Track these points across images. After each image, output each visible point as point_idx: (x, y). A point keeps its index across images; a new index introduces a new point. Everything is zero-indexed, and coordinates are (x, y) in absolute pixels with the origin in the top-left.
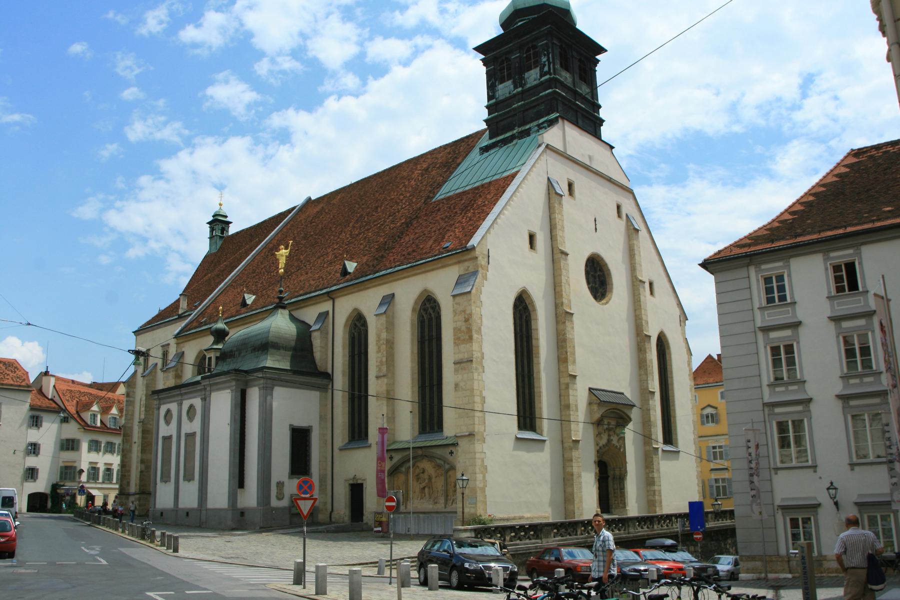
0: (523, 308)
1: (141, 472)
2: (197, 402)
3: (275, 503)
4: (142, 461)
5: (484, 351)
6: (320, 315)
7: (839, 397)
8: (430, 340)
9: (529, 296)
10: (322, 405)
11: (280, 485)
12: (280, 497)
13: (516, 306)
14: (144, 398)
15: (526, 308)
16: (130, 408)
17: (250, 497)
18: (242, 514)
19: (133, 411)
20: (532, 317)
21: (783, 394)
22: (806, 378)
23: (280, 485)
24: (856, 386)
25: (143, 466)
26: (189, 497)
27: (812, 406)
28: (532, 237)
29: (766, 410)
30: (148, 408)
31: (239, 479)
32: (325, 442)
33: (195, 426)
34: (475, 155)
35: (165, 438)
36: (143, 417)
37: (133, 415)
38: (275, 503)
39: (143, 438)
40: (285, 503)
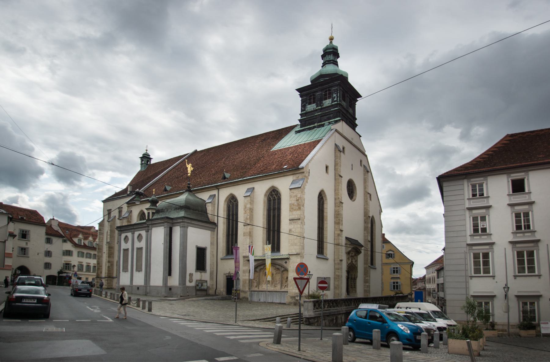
0: (321, 197)
1: (109, 267)
2: (143, 233)
3: (188, 284)
4: (109, 262)
5: (305, 215)
6: (211, 196)
7: (511, 242)
8: (274, 209)
9: (324, 193)
10: (212, 238)
11: (191, 275)
12: (191, 281)
13: (319, 197)
14: (109, 232)
15: (322, 198)
16: (101, 236)
17: (174, 281)
18: (170, 289)
19: (103, 238)
20: (325, 202)
21: (478, 240)
22: (491, 233)
23: (191, 275)
24: (520, 237)
25: (109, 264)
26: (139, 279)
27: (495, 247)
28: (327, 167)
29: (468, 247)
30: (112, 236)
31: (169, 271)
32: (213, 255)
33: (143, 244)
34: (293, 132)
35: (124, 250)
36: (109, 240)
37: (103, 239)
38: (188, 284)
39: (109, 250)
40: (193, 284)
